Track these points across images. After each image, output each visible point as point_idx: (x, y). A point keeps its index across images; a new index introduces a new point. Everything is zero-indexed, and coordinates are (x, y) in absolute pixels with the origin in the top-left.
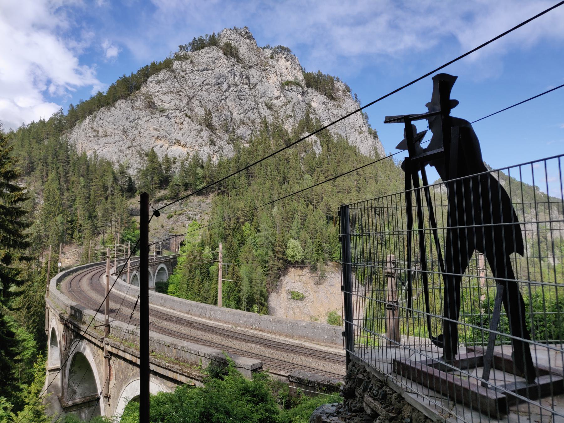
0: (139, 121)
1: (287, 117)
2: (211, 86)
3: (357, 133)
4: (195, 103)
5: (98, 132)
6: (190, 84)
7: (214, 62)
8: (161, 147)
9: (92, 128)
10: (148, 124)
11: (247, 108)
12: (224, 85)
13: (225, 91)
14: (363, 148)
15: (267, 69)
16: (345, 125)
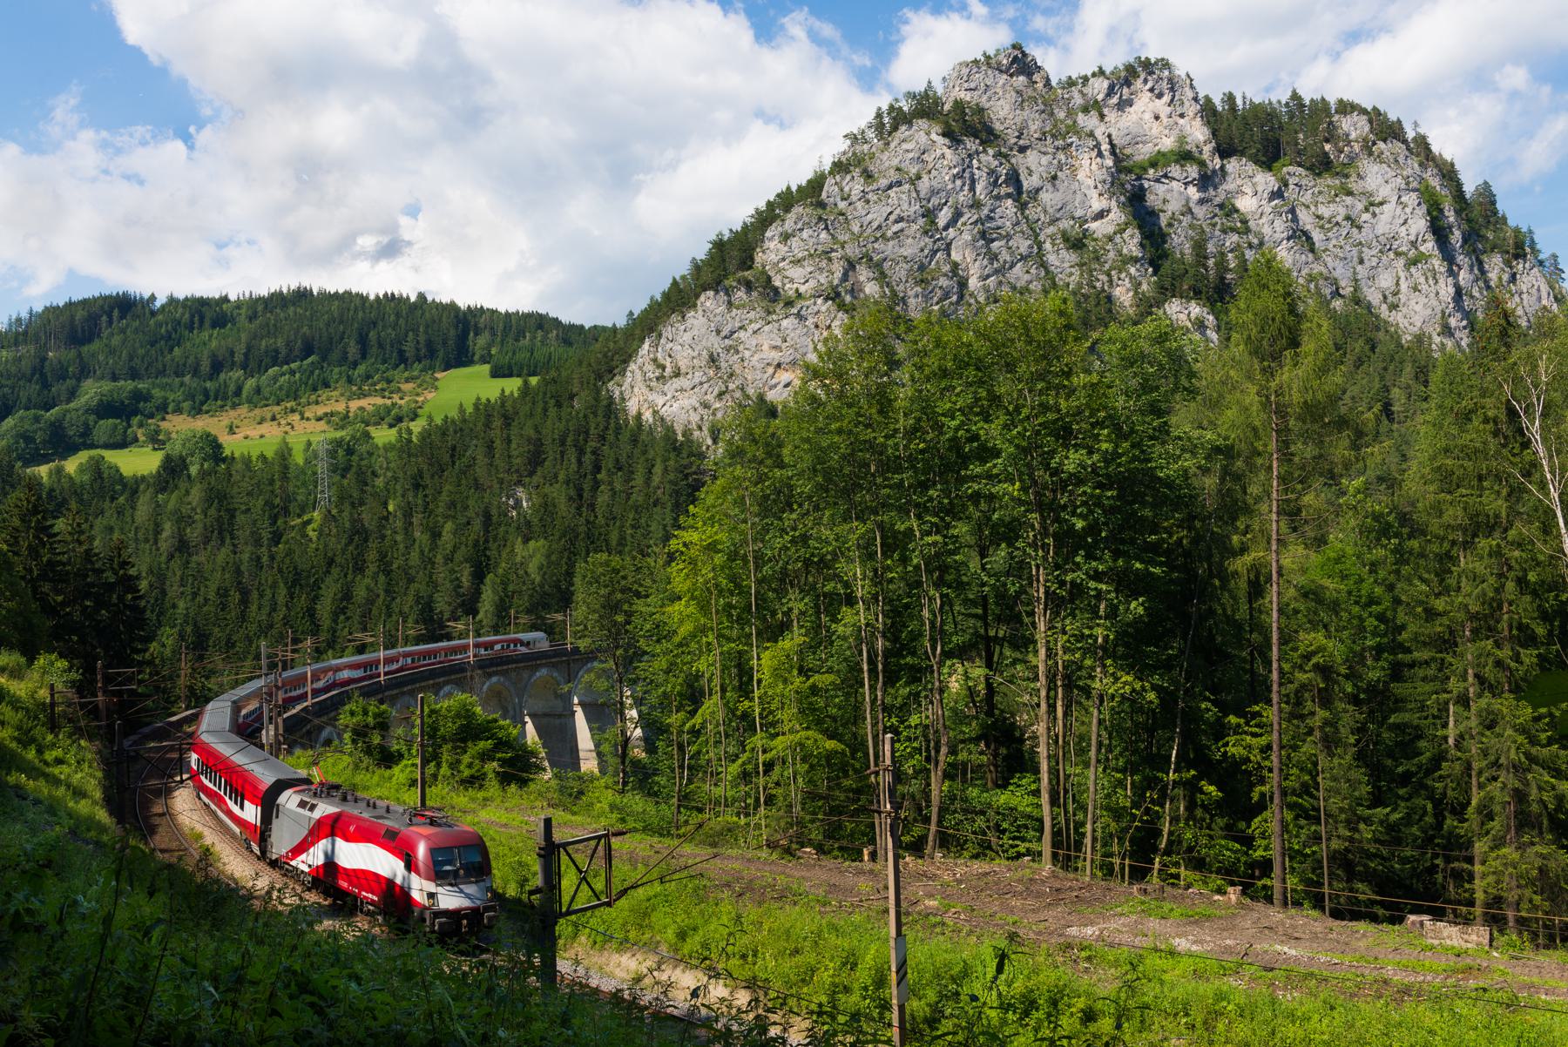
0: (742, 334)
1: (1125, 262)
2: (908, 221)
3: (1401, 262)
4: (863, 273)
5: (664, 370)
6: (856, 229)
7: (920, 160)
8: (787, 386)
9: (655, 360)
10: (760, 338)
11: (1008, 259)
12: (943, 212)
13: (946, 228)
14: (1417, 308)
15: (1070, 145)
16: (1360, 243)
